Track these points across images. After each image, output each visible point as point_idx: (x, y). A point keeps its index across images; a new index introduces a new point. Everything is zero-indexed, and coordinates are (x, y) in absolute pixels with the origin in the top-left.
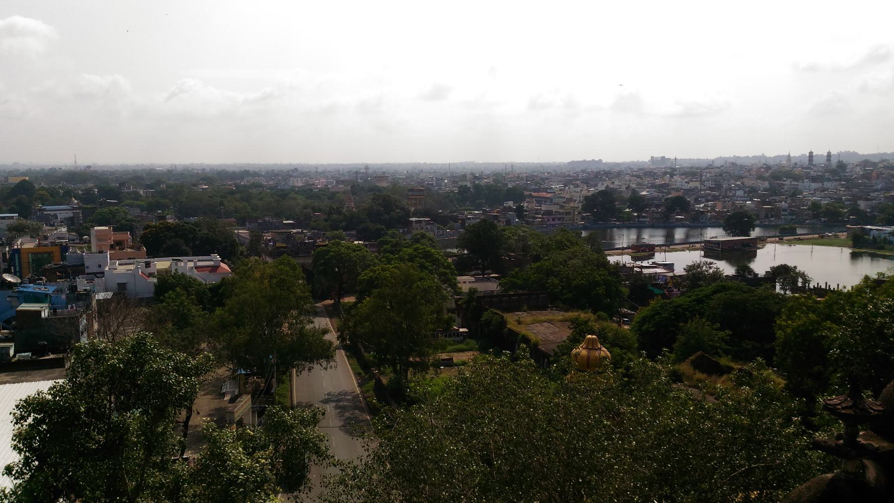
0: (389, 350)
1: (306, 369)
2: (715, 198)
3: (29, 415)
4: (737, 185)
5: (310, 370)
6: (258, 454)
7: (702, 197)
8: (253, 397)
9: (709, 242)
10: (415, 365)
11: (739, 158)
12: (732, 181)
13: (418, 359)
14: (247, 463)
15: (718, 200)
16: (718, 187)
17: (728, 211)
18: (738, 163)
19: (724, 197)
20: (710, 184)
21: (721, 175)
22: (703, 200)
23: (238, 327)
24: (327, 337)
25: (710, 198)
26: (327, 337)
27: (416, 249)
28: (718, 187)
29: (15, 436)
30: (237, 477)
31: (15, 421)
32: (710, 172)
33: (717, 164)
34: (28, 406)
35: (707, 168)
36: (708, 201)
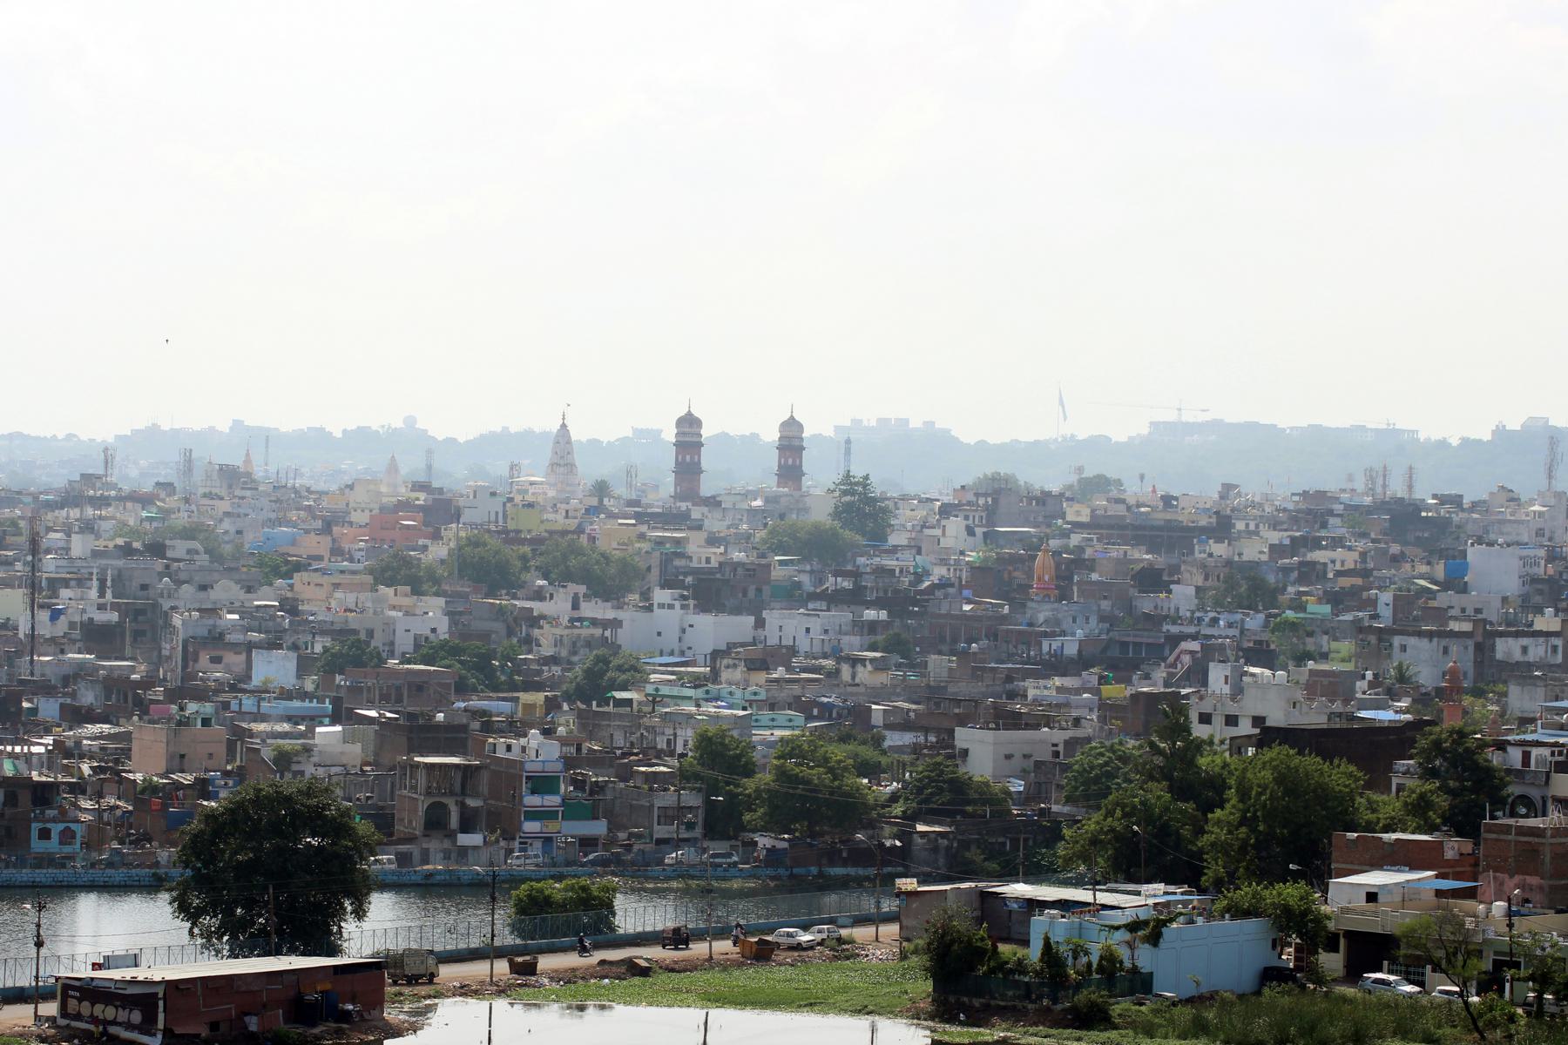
2: (125, 699)
7: (46, 689)
11: (268, 438)
12: (226, 590)
15: (142, 707)
16: (140, 623)
17: (203, 788)
19: (174, 695)
20: (86, 603)
22: (49, 708)
25: (88, 697)
28: (140, 623)
32: (88, 527)
33: (134, 474)
35: (70, 498)
36: (77, 716)
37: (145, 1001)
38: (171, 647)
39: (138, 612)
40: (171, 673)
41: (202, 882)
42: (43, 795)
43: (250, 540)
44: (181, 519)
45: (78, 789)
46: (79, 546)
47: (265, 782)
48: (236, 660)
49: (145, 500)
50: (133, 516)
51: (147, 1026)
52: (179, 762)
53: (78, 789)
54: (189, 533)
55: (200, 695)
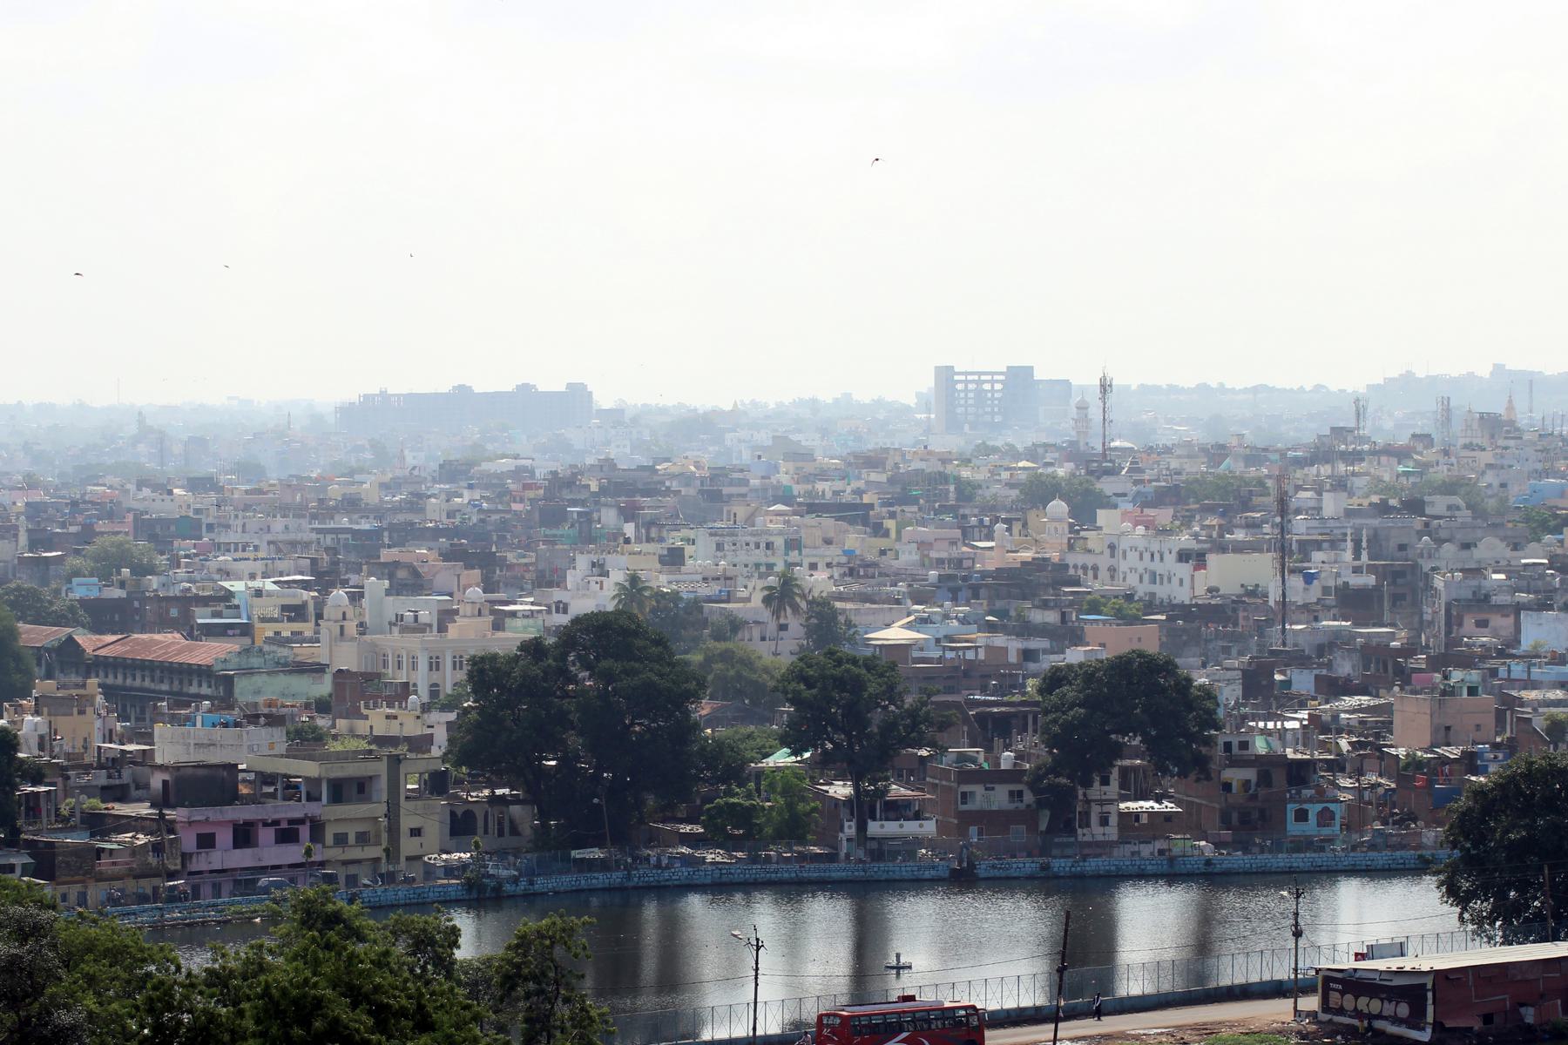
2: (1384, 668)
4: (1522, 577)
7: (1299, 659)
9: (1352, 983)
11: (1531, 382)
12: (1490, 548)
15: (1404, 677)
16: (1400, 585)
17: (1471, 762)
18: (1527, 416)
19: (1440, 662)
20: (1339, 567)
21: (1414, 506)
22: (1303, 681)
25: (1345, 667)
28: (1400, 585)
32: (1340, 485)
33: (1387, 426)
35: (1321, 454)
36: (1334, 687)
37: (1411, 991)
38: (1434, 610)
39: (1396, 575)
40: (1433, 639)
41: (1470, 863)
42: (1299, 773)
43: (1515, 493)
44: (1441, 473)
45: (1337, 766)
46: (1331, 505)
47: (1537, 756)
48: (1503, 623)
49: (1401, 454)
50: (1388, 471)
51: (1415, 1020)
52: (1445, 734)
53: (1337, 766)
54: (1449, 488)
55: (1466, 662)
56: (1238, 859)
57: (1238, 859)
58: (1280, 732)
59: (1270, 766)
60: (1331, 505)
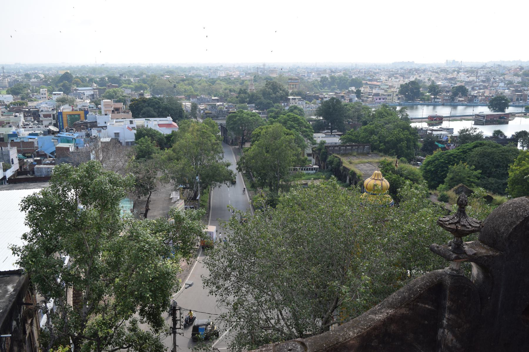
0: (267, 176)
1: (217, 186)
2: (485, 87)
3: (29, 206)
4: (500, 79)
5: (219, 187)
6: (157, 234)
7: (477, 86)
8: (185, 201)
9: (478, 115)
10: (282, 186)
11: (503, 62)
12: (497, 77)
13: (284, 183)
14: (151, 239)
15: (487, 88)
16: (488, 80)
17: (492, 96)
18: (503, 65)
19: (490, 87)
20: (482, 78)
21: (490, 73)
22: (477, 88)
23: (178, 160)
24: (229, 168)
25: (481, 87)
26: (229, 168)
27: (289, 116)
28: (488, 80)
29: (27, 217)
30: (144, 246)
31: (21, 209)
32: (483, 71)
33: (489, 65)
34: (29, 201)
35: (482, 68)
36: (480, 89)
37: (484, 116)
38: (491, 82)
39: (487, 79)
40: (491, 85)
41: (491, 105)
42: (476, 97)
43: (500, 72)
44: (493, 70)
45: (480, 96)
46: (482, 73)
47: (498, 95)
48: (497, 84)
49: (490, 68)
50: (488, 70)
51: (484, 119)
52: (490, 93)
53: (480, 96)
54: (494, 71)
55: (493, 87)
56: (469, 104)
57: (469, 104)
58: (474, 93)
59: (473, 96)
60: (482, 73)
